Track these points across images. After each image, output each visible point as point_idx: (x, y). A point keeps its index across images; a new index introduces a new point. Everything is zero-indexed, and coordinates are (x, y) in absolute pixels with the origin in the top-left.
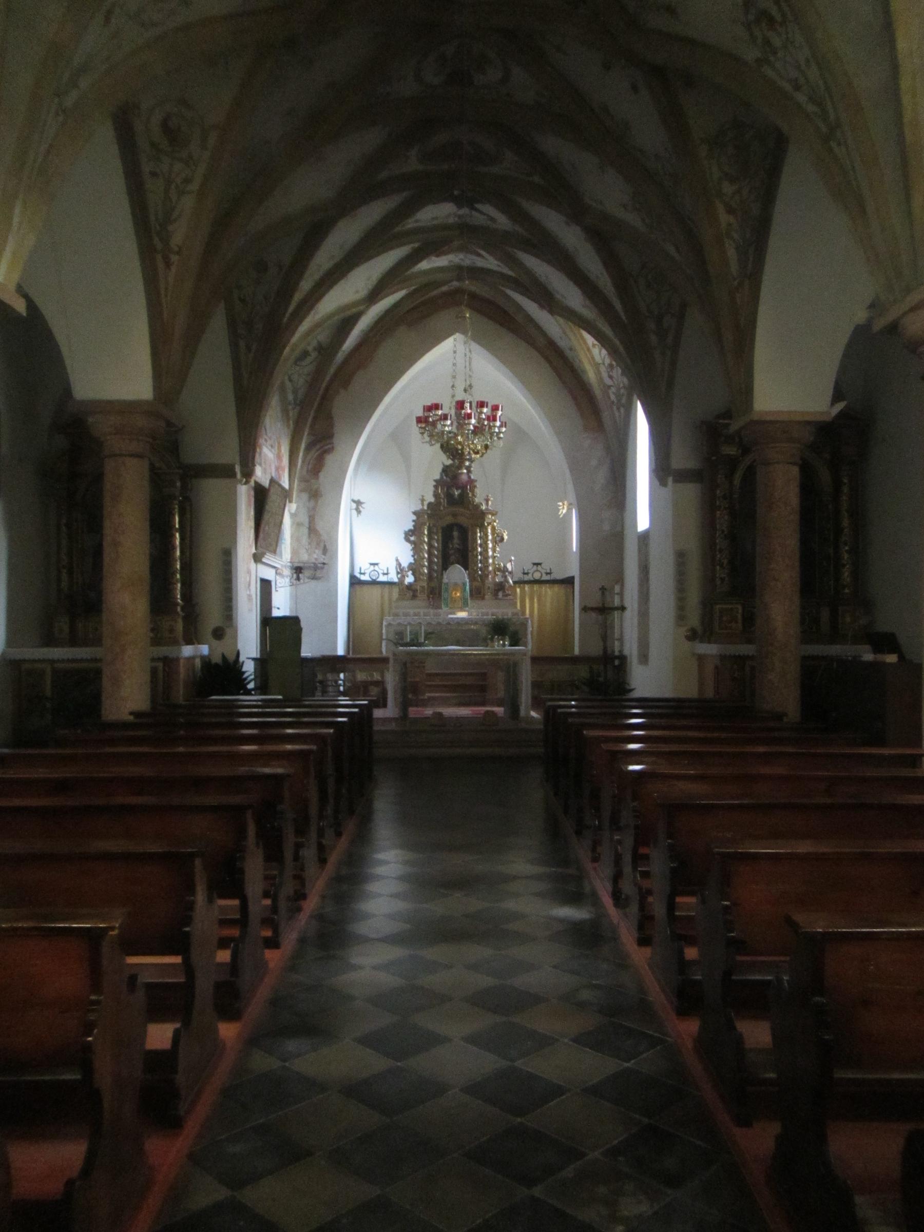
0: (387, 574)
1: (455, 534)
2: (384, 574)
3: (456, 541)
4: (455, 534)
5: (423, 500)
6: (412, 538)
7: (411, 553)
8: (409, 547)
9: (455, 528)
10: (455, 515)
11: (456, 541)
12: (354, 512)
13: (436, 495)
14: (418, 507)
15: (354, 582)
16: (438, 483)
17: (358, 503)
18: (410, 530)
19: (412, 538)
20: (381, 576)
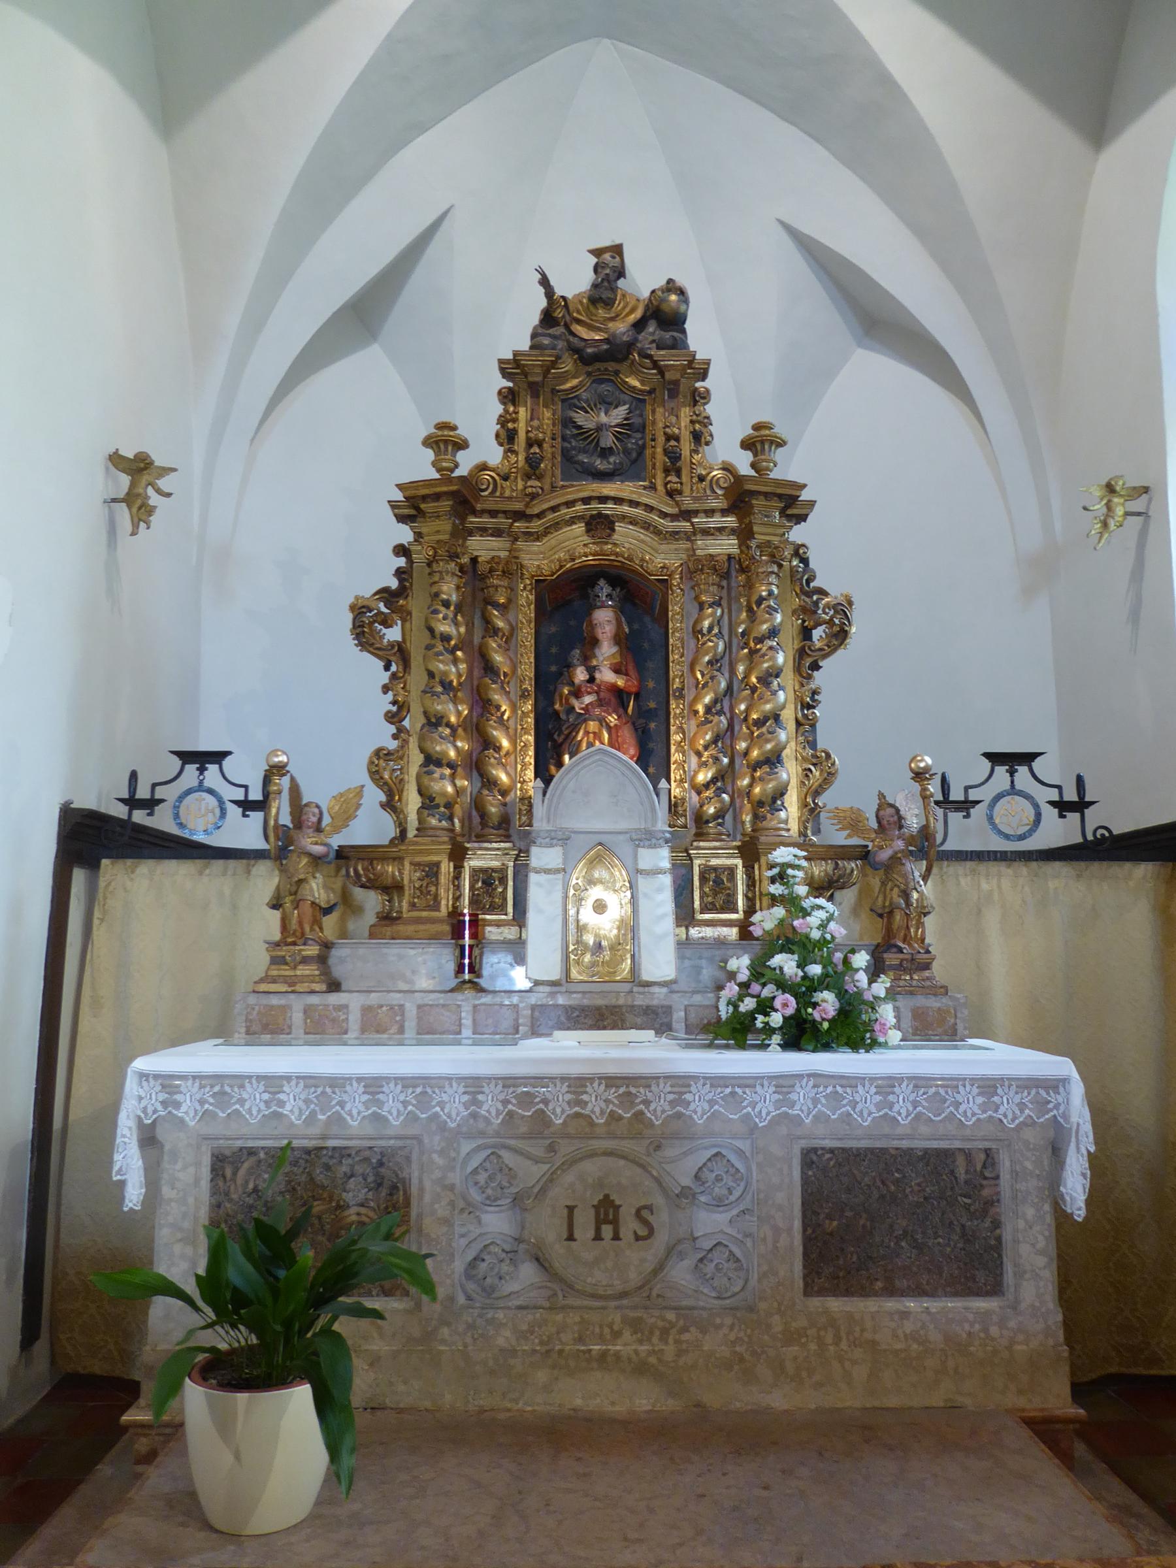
0: (261, 805)
1: (605, 619)
2: (247, 806)
3: (607, 651)
4: (605, 619)
5: (445, 441)
6: (393, 634)
7: (385, 703)
8: (374, 671)
9: (603, 589)
10: (600, 525)
11: (607, 651)
12: (123, 514)
13: (507, 437)
14: (422, 467)
15: (88, 840)
16: (523, 379)
17: (139, 467)
18: (385, 594)
19: (393, 634)
20: (234, 812)
